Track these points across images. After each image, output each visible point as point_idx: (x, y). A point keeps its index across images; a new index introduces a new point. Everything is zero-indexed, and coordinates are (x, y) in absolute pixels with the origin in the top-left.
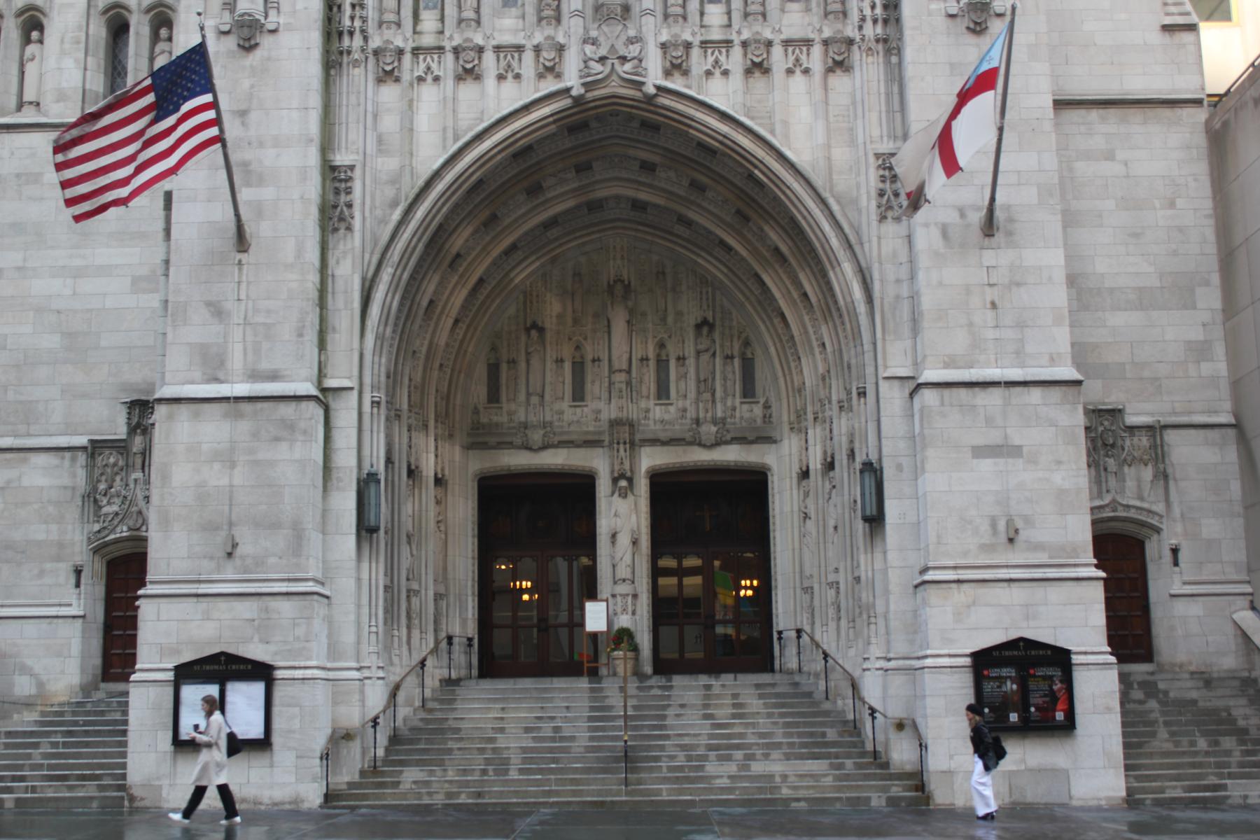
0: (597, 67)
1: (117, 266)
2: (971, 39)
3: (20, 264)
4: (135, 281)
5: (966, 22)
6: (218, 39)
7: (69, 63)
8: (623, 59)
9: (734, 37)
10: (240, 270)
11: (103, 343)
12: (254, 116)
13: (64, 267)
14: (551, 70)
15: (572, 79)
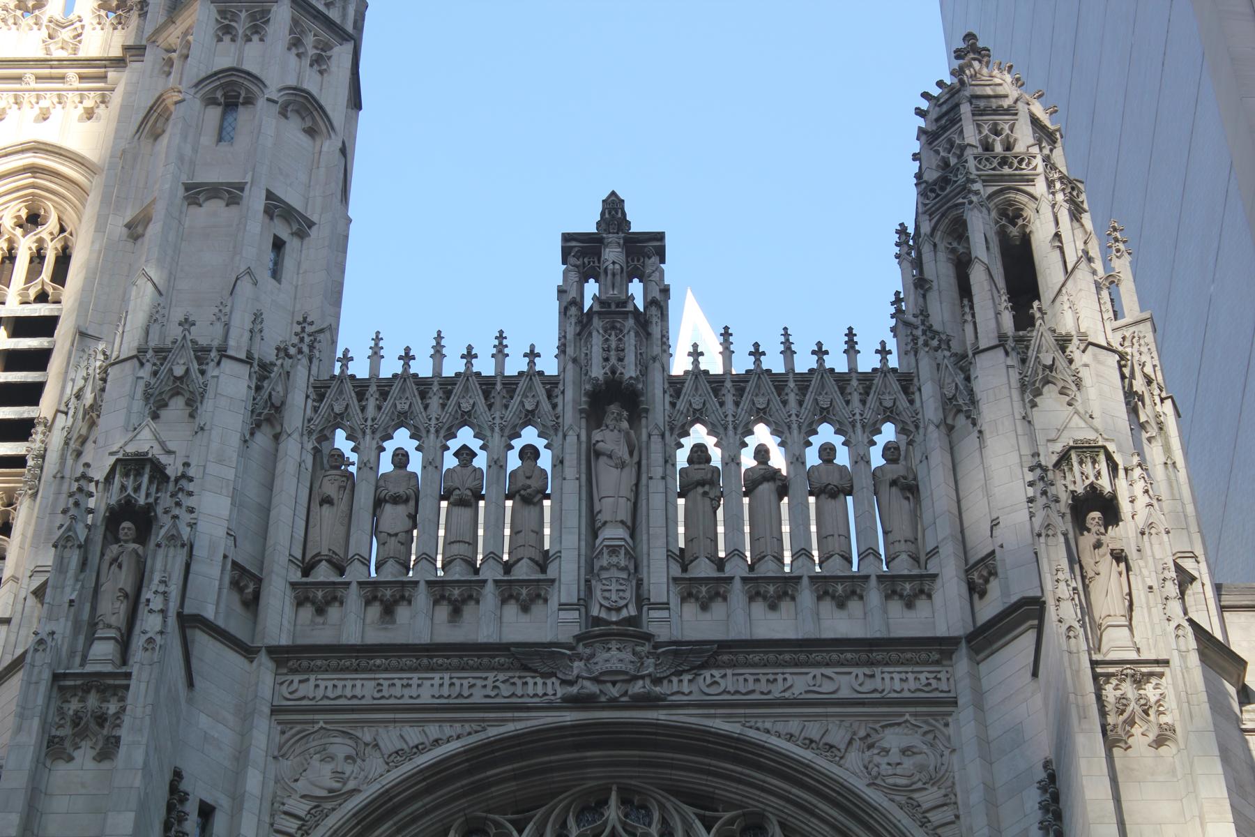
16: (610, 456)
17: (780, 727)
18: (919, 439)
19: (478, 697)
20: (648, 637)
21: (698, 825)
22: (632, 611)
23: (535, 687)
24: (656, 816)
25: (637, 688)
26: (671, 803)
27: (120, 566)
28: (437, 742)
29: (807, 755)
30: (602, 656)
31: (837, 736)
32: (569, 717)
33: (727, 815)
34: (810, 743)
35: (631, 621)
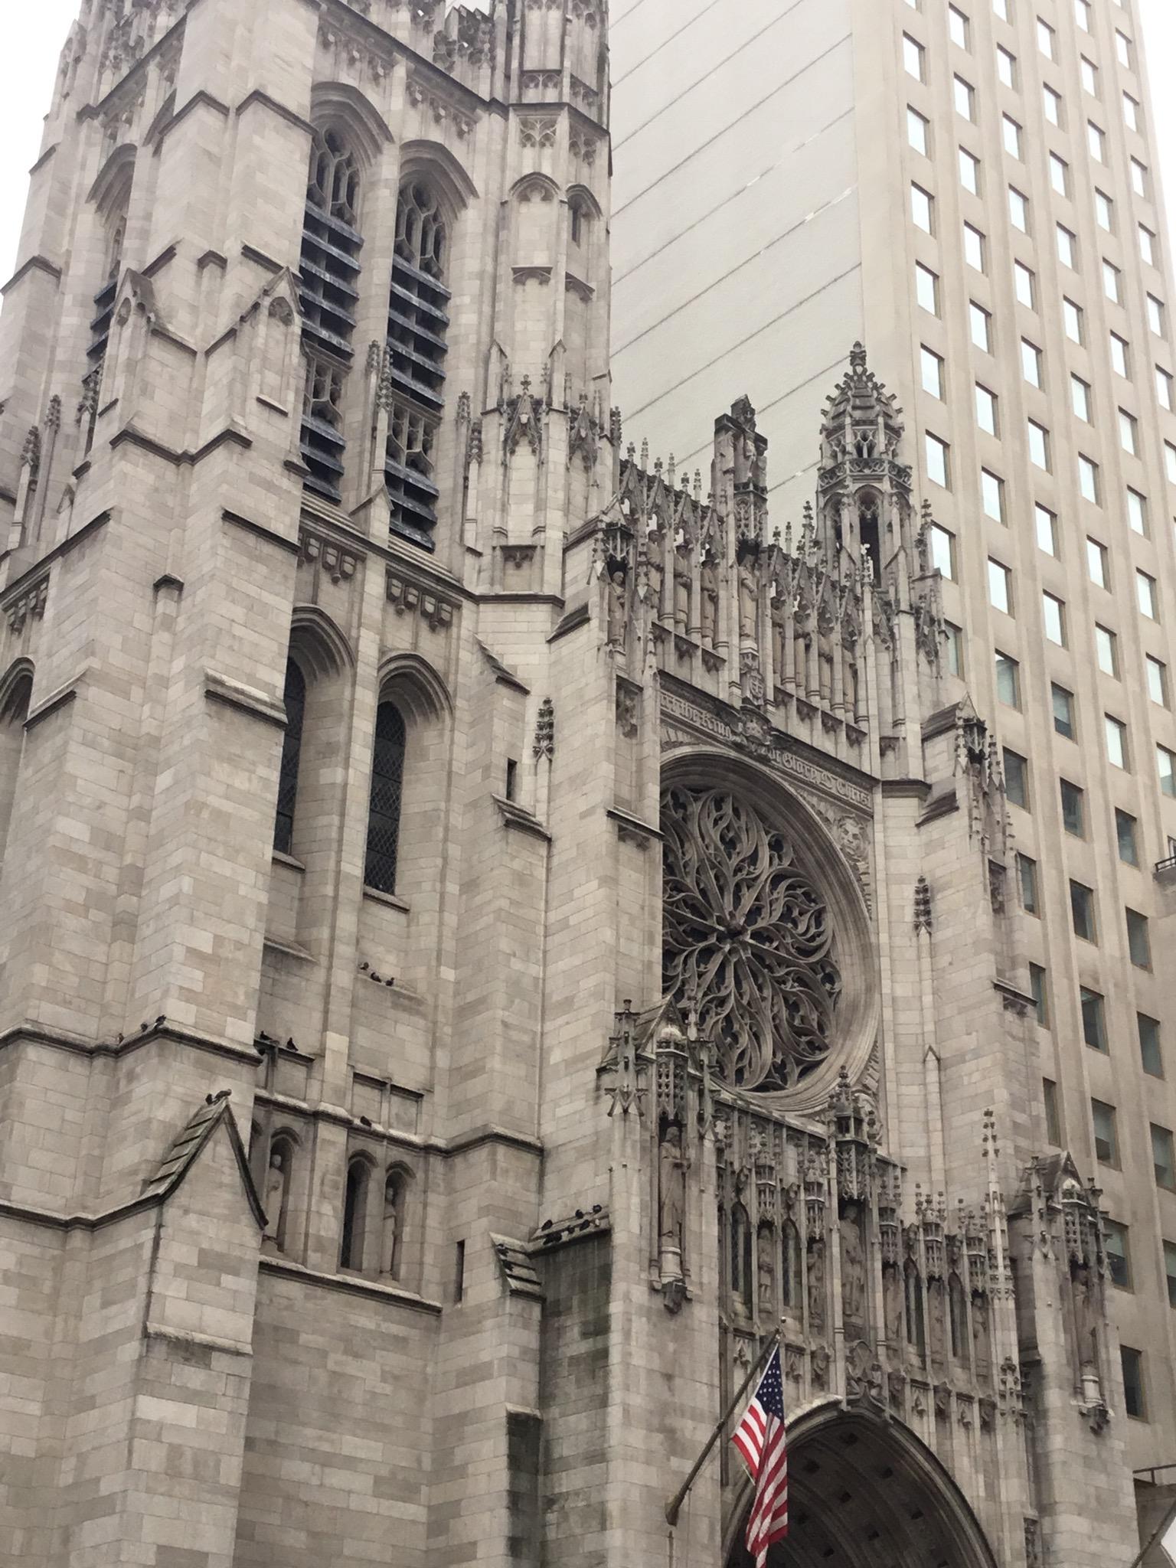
0: (857, 1389)
1: (361, 1460)
2: (1092, 1436)
3: (273, 1437)
4: (378, 1481)
5: (1092, 1422)
6: (650, 1294)
7: (327, 1209)
8: (871, 1384)
9: (929, 1381)
10: (671, 1544)
11: (346, 1552)
12: (678, 1381)
13: (313, 1450)
14: (820, 1381)
15: (838, 1393)
16: (751, 592)
17: (809, 798)
18: (861, 641)
19: (697, 724)
20: (767, 721)
21: (763, 833)
22: (761, 702)
23: (721, 729)
24: (743, 818)
25: (763, 751)
26: (752, 815)
27: (622, 605)
28: (681, 744)
29: (817, 818)
30: (750, 725)
31: (830, 815)
32: (733, 754)
33: (774, 832)
34: (819, 813)
35: (758, 707)
